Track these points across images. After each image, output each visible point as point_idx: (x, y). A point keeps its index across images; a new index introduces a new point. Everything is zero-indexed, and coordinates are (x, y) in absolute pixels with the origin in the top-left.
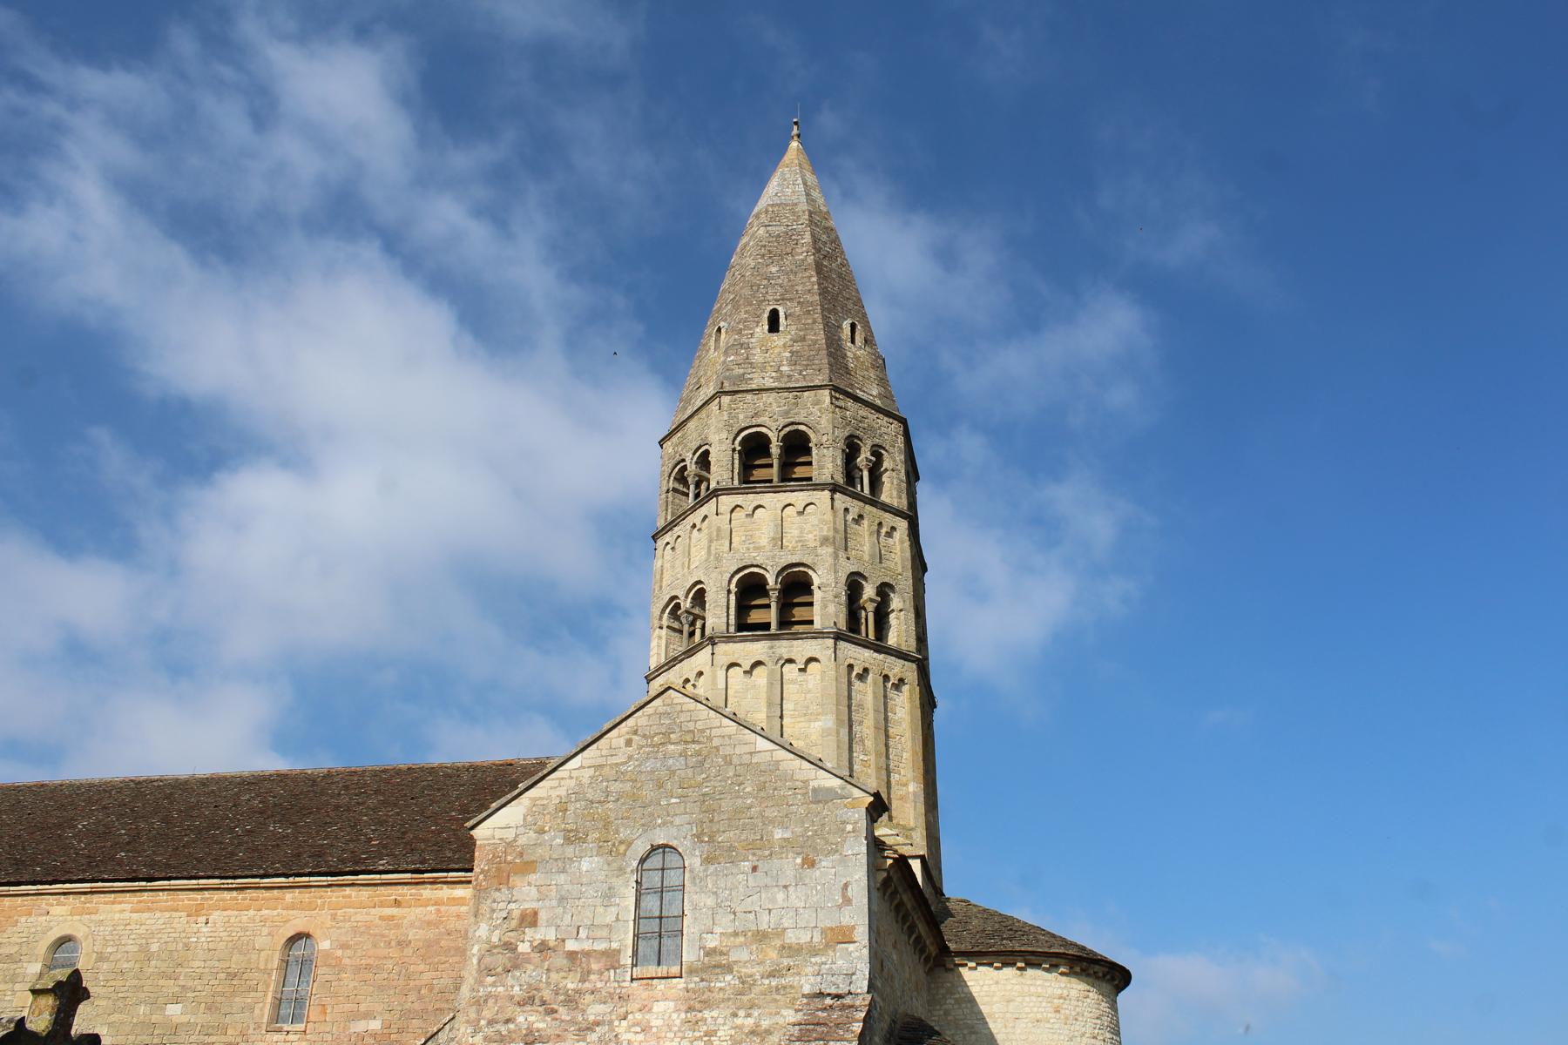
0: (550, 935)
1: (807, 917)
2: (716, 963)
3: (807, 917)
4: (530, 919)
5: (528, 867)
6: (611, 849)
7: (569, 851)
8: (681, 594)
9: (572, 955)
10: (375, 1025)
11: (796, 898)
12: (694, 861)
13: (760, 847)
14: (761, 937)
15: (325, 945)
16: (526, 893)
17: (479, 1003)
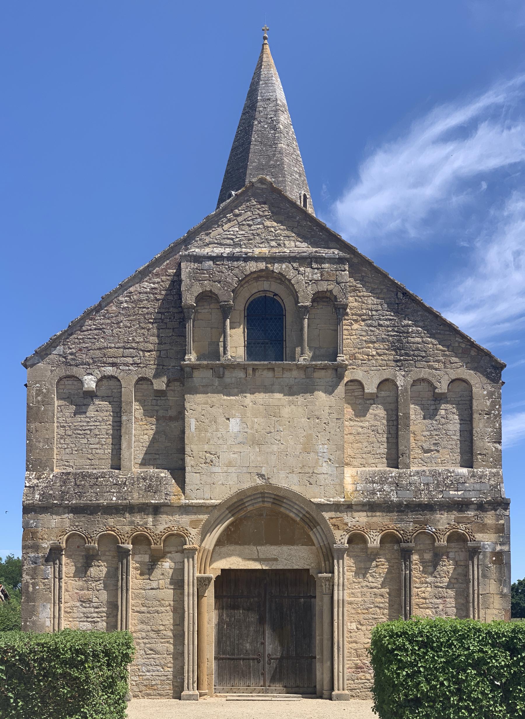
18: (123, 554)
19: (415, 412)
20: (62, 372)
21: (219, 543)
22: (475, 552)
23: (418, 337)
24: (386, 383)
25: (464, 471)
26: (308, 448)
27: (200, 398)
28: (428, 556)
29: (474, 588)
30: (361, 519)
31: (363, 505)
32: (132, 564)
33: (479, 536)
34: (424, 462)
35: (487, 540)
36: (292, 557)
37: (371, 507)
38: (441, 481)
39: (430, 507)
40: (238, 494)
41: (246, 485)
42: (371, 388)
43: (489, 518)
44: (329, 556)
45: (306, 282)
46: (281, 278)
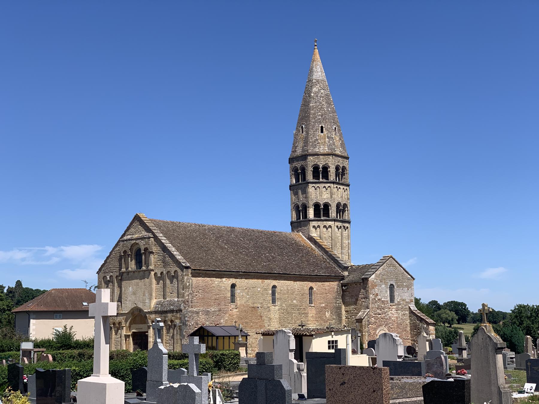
0: (380, 297)
1: (408, 298)
2: (399, 304)
3: (408, 298)
4: (377, 295)
5: (376, 286)
6: (386, 284)
7: (381, 283)
8: (322, 203)
9: (383, 301)
10: (324, 305)
11: (406, 294)
12: (395, 287)
13: (403, 286)
14: (403, 300)
15: (315, 289)
16: (376, 290)
17: (373, 308)
18: (111, 328)
19: (168, 282)
20: (103, 275)
21: (131, 324)
22: (175, 326)
23: (168, 259)
24: (162, 273)
25: (176, 299)
26: (144, 295)
27: (124, 282)
28: (168, 327)
29: (175, 337)
30: (153, 316)
31: (154, 311)
32: (113, 331)
33: (176, 321)
34: (171, 297)
35: (177, 322)
36: (142, 328)
37: (156, 312)
38: (171, 303)
39: (166, 312)
40: (132, 309)
41: (133, 307)
42: (159, 275)
43: (178, 315)
44: (149, 327)
45: (142, 244)
46: (137, 244)
